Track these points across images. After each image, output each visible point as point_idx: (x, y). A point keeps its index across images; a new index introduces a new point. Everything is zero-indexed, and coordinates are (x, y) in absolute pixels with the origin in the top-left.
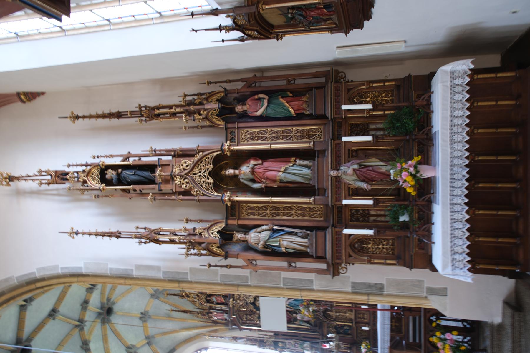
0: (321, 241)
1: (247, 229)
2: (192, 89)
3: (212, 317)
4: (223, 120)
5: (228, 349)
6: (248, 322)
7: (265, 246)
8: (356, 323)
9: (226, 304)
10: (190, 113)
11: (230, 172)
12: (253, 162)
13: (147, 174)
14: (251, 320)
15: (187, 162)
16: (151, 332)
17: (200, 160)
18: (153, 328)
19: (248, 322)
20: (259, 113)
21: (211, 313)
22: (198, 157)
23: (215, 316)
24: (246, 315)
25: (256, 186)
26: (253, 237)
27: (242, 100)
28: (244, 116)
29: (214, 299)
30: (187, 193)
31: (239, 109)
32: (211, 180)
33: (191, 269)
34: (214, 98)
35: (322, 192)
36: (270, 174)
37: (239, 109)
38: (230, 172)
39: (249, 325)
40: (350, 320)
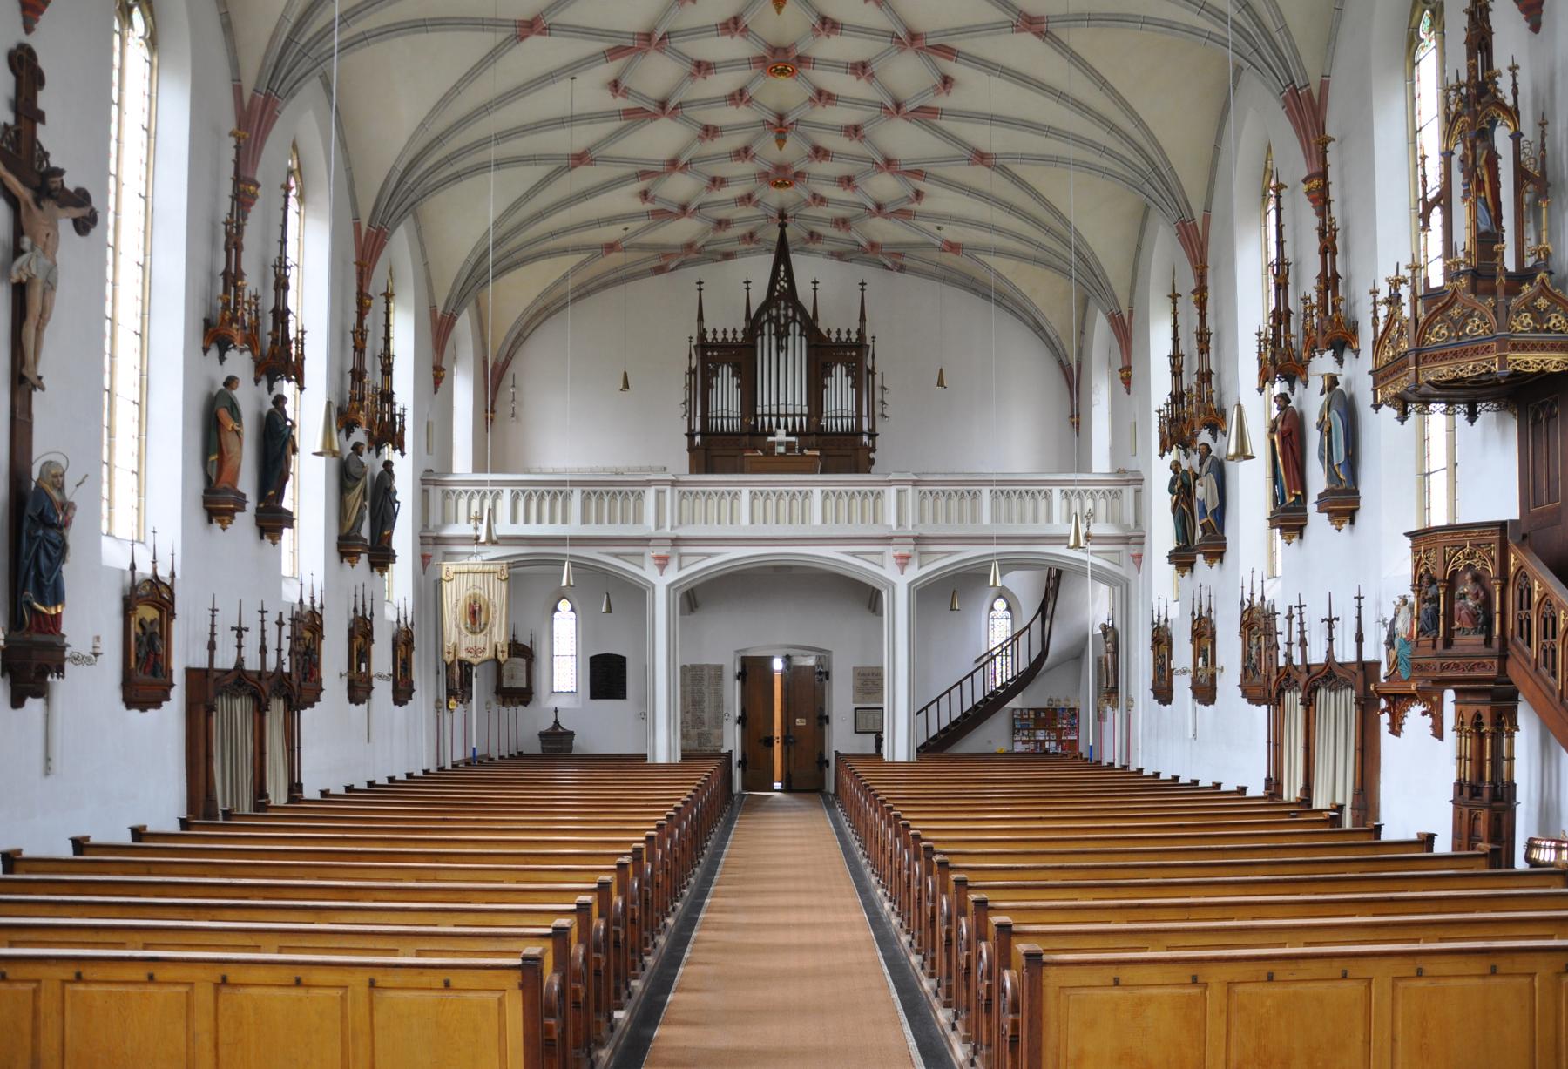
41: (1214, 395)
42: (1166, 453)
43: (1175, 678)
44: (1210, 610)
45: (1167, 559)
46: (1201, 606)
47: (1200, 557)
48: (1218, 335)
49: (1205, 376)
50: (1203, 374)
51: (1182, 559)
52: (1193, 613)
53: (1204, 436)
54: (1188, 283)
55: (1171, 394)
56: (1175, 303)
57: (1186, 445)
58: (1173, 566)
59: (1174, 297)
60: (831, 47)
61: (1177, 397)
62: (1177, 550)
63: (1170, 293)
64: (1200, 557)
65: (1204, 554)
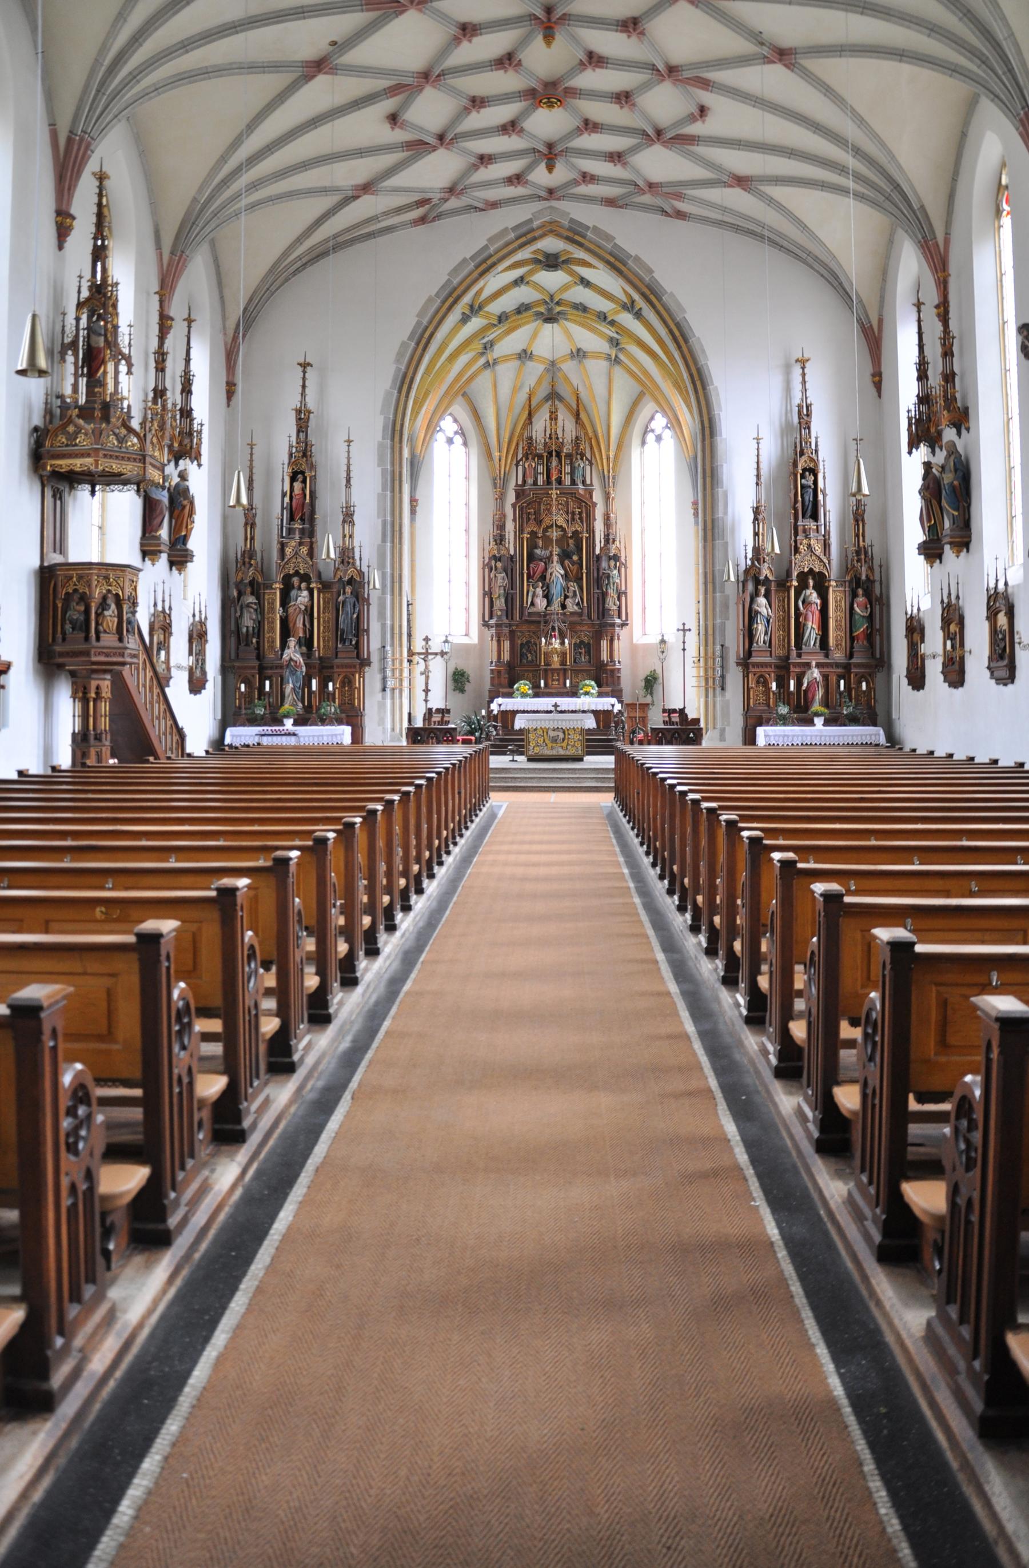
0: (764, 654)
1: (767, 596)
2: (876, 551)
3: (527, 459)
4: (852, 579)
5: (467, 478)
6: (525, 516)
7: (757, 612)
8: (546, 671)
9: (548, 481)
10: (858, 553)
11: (811, 583)
12: (818, 601)
13: (809, 513)
14: (529, 519)
15: (818, 549)
16: (500, 368)
17: (821, 561)
18: (506, 372)
19: (525, 516)
20: (857, 609)
21: (533, 459)
22: (826, 561)
23: (530, 465)
24: (535, 513)
25: (800, 603)
26: (762, 600)
27: (868, 594)
28: (854, 595)
29: (554, 462)
30: (797, 550)
31: (860, 591)
32: (806, 570)
33: (727, 543)
34: (870, 574)
35: (799, 656)
36: (810, 614)
37: (860, 591)
38: (811, 583)
39: (521, 517)
40: (547, 664)
41: (957, 395)
42: (914, 450)
43: (927, 662)
44: (958, 597)
45: (917, 551)
46: (950, 594)
47: (947, 547)
48: (961, 339)
49: (949, 377)
50: (947, 375)
51: (931, 551)
52: (942, 602)
53: (949, 434)
54: (931, 296)
55: (918, 396)
56: (919, 311)
57: (933, 441)
58: (922, 557)
59: (919, 305)
60: (591, 79)
61: (923, 399)
62: (924, 542)
63: (915, 301)
64: (947, 547)
65: (950, 543)
